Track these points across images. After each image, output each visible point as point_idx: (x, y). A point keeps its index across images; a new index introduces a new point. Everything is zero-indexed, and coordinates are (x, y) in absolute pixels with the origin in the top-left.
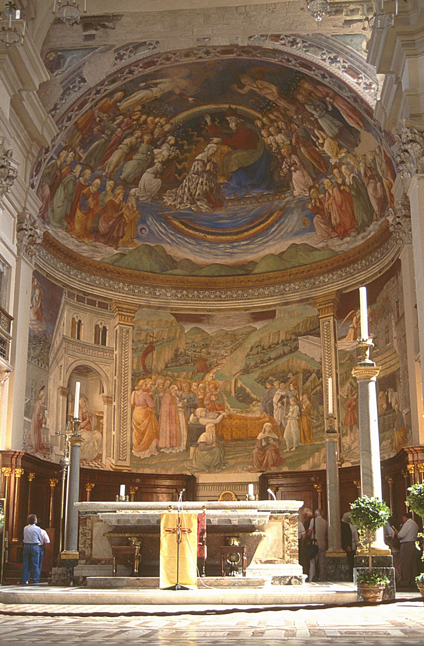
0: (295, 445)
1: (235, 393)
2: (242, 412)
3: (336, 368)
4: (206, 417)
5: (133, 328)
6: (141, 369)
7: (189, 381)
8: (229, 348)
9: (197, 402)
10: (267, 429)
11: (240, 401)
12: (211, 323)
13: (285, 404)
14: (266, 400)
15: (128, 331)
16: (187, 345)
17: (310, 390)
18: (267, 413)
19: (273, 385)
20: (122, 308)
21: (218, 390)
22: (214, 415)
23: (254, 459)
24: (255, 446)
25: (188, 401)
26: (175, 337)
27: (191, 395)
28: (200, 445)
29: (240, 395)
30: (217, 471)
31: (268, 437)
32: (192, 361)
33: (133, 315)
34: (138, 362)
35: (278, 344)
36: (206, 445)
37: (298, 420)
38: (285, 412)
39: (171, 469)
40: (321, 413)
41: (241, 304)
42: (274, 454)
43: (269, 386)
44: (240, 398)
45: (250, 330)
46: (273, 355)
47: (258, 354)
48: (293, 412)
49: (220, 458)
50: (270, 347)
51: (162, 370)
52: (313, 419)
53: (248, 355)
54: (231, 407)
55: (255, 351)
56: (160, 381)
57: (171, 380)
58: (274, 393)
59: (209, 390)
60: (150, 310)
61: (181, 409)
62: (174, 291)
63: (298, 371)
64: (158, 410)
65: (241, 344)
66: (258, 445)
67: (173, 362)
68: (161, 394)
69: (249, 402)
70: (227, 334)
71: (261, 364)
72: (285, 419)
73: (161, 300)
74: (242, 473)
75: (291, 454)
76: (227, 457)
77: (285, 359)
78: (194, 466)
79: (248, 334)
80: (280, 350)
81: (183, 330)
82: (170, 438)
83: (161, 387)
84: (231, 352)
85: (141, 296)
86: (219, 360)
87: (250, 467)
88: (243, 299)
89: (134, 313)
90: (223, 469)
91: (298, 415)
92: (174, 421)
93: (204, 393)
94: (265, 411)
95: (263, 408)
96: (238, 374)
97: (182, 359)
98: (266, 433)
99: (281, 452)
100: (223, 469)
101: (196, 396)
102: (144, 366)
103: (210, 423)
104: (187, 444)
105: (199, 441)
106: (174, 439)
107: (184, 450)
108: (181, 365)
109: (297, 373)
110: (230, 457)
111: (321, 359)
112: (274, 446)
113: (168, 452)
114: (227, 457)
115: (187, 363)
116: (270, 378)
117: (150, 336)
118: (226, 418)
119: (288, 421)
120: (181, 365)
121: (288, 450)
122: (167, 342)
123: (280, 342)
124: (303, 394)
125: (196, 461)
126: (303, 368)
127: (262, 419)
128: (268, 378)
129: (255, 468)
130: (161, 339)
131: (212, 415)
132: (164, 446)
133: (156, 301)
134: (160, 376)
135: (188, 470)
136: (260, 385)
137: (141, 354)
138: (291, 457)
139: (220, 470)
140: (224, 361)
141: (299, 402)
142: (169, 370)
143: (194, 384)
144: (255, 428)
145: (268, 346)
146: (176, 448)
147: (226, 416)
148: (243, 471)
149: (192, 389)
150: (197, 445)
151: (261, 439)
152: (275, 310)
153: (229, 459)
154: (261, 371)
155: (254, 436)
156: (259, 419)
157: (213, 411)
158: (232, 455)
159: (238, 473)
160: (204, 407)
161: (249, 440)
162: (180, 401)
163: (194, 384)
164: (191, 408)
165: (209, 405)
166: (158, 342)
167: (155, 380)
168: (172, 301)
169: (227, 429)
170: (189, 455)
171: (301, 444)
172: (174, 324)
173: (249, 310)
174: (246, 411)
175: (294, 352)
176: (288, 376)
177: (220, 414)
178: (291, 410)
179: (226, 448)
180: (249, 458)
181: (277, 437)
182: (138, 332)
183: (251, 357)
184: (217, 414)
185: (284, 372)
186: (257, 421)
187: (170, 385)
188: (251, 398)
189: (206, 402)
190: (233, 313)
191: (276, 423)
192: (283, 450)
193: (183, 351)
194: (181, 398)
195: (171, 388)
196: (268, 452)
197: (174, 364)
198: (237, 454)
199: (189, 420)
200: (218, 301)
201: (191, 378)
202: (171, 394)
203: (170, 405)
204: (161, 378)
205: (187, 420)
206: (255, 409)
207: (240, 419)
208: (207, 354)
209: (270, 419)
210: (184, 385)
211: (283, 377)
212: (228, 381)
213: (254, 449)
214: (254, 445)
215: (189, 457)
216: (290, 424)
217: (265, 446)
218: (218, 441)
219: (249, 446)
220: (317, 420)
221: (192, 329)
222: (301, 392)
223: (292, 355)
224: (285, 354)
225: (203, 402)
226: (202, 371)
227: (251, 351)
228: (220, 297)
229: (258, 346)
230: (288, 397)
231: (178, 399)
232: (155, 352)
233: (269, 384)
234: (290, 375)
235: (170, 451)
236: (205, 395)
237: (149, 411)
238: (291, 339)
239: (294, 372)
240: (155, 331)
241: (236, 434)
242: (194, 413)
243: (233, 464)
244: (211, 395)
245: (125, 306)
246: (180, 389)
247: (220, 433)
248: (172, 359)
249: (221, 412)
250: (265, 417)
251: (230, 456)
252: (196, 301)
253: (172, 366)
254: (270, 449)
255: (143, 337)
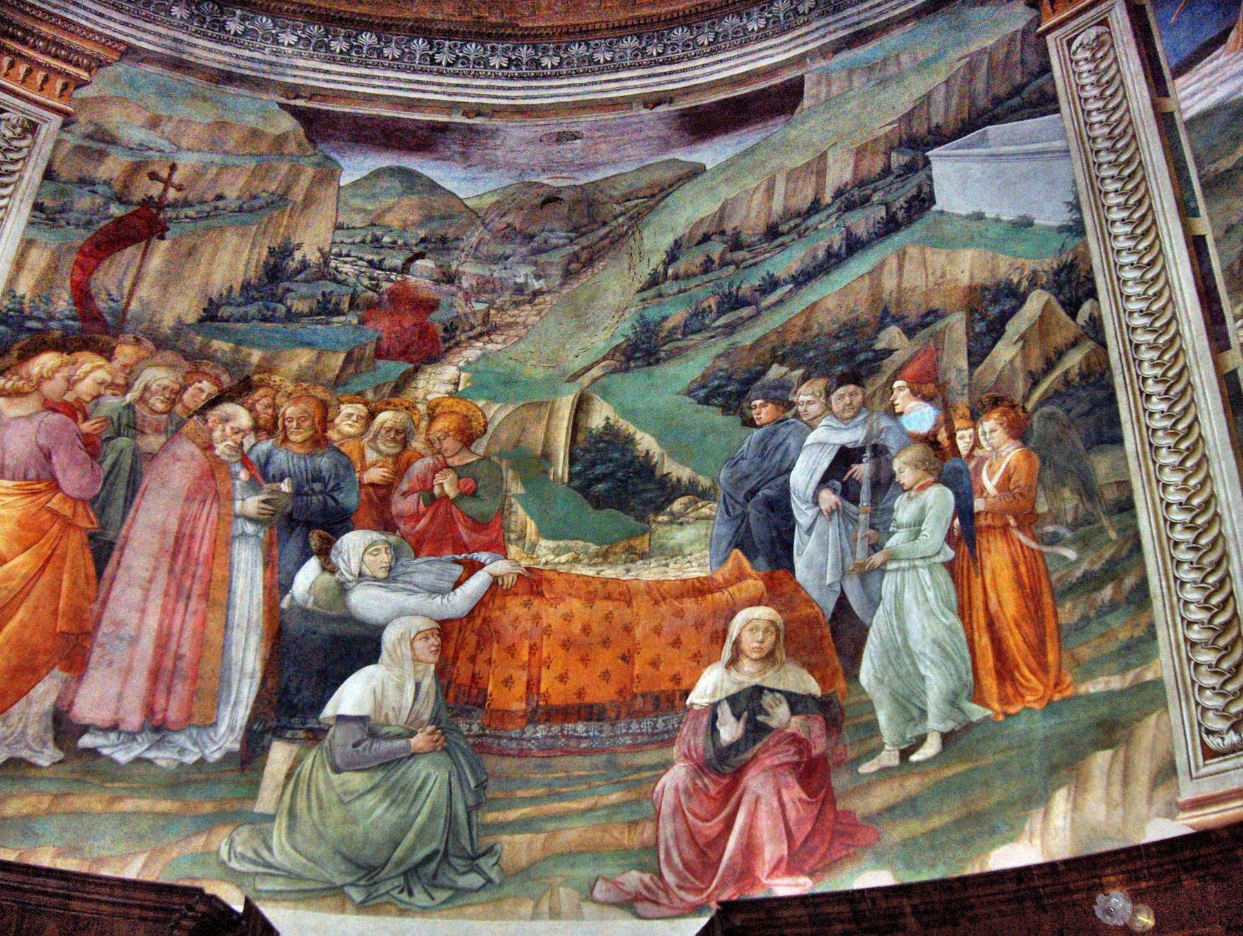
0: (935, 725)
1: (572, 459)
2: (605, 556)
3: (1186, 211)
4: (390, 577)
5: (65, 125)
6: (63, 303)
7: (326, 396)
8: (557, 257)
9: (350, 499)
10: (750, 643)
11: (599, 503)
12: (476, 157)
13: (865, 490)
14: (749, 485)
15: (31, 128)
16: (340, 236)
17: (1020, 386)
18: (750, 553)
19: (791, 405)
20: (27, 31)
21: (481, 447)
22: (440, 576)
23: (667, 829)
24: (675, 751)
25: (298, 492)
26: (283, 197)
27: (324, 462)
28: (339, 737)
29: (599, 470)
30: (420, 898)
31: (758, 690)
32: (353, 305)
33: (85, 75)
34: (53, 267)
35: (816, 207)
36: (373, 735)
37: (950, 566)
38: (862, 531)
39: (124, 859)
40: (1111, 495)
41: (633, 83)
42: (793, 793)
43: (763, 412)
44: (600, 487)
45: (668, 175)
46: (786, 262)
47: (706, 271)
48: (916, 528)
49: (451, 819)
50: (772, 232)
51: (180, 328)
52: (1055, 540)
53: (654, 281)
54: (544, 533)
55: (691, 261)
56: (158, 376)
57: (225, 378)
58: (792, 442)
59: (430, 442)
60: (177, 75)
61: (250, 528)
62: (314, 30)
63: (936, 303)
64: (114, 513)
65: (616, 241)
66: (692, 738)
67: (249, 301)
68: (152, 442)
69: (651, 501)
70: (552, 199)
71: (721, 313)
72: (869, 575)
73: (247, 53)
74: (578, 915)
75: (913, 784)
76: (491, 817)
77: (859, 266)
78: (278, 858)
79: (659, 194)
80: (827, 233)
81: (328, 173)
82: (155, 674)
83: (160, 406)
84: (568, 275)
85: (147, 19)
86: (501, 309)
87: (633, 879)
88: (640, 66)
89: (88, 69)
90: (459, 892)
91: (950, 539)
92: (197, 589)
93: (397, 457)
94: (742, 541)
95: (724, 531)
96: (596, 372)
97: (304, 289)
98: (747, 665)
99: (840, 781)
100: (459, 892)
101: (349, 466)
102: (82, 295)
103: (415, 614)
104: (252, 719)
105: (329, 711)
106: (181, 689)
107: (229, 756)
108: (291, 316)
109: (932, 315)
110: (513, 815)
111: (1076, 207)
112: (795, 739)
113: (122, 757)
114: (491, 817)
115: (326, 309)
116: (776, 371)
117: (153, 176)
118: (506, 593)
119: (888, 586)
120: (291, 316)
121: (889, 757)
122: (241, 210)
123: (827, 198)
124: (975, 417)
125: (291, 829)
126: (965, 280)
127: (719, 588)
128: (763, 373)
129: (666, 889)
130: (210, 196)
131: (425, 570)
132: (102, 716)
133: (220, 52)
134: (169, 356)
135: (234, 877)
136: (713, 416)
137: (80, 237)
138: (909, 807)
139: (441, 895)
140: (526, 314)
141: (951, 463)
142: (224, 334)
143: (346, 409)
144: (676, 643)
145: (761, 228)
146: (181, 739)
147: (509, 581)
148: (588, 908)
149: (332, 434)
150: (316, 735)
151: (715, 706)
152: (802, 78)
153: (505, 827)
154: (723, 345)
155: (667, 686)
156: (699, 589)
157: (436, 552)
158: (524, 801)
159: (555, 914)
160: (386, 524)
161: (639, 715)
162: (254, 485)
163: (346, 409)
164: (309, 525)
165: (417, 517)
166: (187, 203)
167: (131, 372)
168: (301, 63)
169: (511, 650)
170: (255, 785)
171: (977, 712)
172: (292, 147)
173: (671, 101)
174: (630, 550)
175: (910, 221)
176: (880, 345)
177: (473, 568)
178: (904, 510)
179: (490, 762)
180: (633, 824)
181: (810, 685)
182: (87, 143)
183: (669, 287)
184: (458, 570)
185: (851, 328)
186: (689, 604)
187: (213, 403)
188: (663, 482)
189: (402, 505)
190: (588, 118)
191: (809, 601)
192: (858, 761)
193: (314, 257)
194: (262, 473)
195: (213, 415)
196: (756, 783)
197: (252, 309)
198: (561, 797)
199: (286, 587)
200: (521, 77)
201: (338, 382)
202: (209, 447)
203: (188, 499)
204: (171, 366)
205: (278, 586)
206: (681, 536)
207: (590, 599)
208: (437, 282)
209: (771, 583)
210: (290, 410)
211: (850, 354)
212: (540, 404)
213: (666, 766)
214: (666, 740)
215: (253, 797)
216: (898, 596)
217: (735, 747)
218: (444, 715)
219: (635, 747)
220: (1083, 543)
221: (377, 174)
222: (962, 404)
223: (898, 239)
224: (854, 246)
225: (385, 501)
226: (404, 354)
227: (672, 257)
228: (537, 64)
229: (706, 238)
230: (879, 451)
231: (244, 475)
232: (164, 245)
233: (767, 399)
234: (892, 336)
235: (137, 750)
236: (401, 466)
237: (55, 514)
238: (887, 171)
239: (913, 314)
240: (187, 161)
241: (563, 678)
242: (324, 553)
243: (523, 860)
244: (436, 471)
245: (45, 29)
246: (267, 427)
247: (463, 671)
248: (246, 286)
249: (483, 556)
250: (741, 576)
251: (511, 806)
252: (415, 71)
253: (244, 319)
254: (768, 762)
255: (112, 167)
